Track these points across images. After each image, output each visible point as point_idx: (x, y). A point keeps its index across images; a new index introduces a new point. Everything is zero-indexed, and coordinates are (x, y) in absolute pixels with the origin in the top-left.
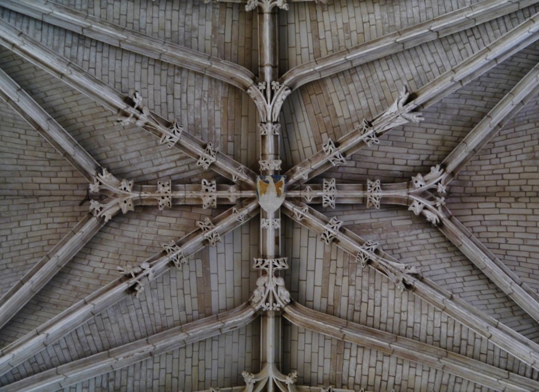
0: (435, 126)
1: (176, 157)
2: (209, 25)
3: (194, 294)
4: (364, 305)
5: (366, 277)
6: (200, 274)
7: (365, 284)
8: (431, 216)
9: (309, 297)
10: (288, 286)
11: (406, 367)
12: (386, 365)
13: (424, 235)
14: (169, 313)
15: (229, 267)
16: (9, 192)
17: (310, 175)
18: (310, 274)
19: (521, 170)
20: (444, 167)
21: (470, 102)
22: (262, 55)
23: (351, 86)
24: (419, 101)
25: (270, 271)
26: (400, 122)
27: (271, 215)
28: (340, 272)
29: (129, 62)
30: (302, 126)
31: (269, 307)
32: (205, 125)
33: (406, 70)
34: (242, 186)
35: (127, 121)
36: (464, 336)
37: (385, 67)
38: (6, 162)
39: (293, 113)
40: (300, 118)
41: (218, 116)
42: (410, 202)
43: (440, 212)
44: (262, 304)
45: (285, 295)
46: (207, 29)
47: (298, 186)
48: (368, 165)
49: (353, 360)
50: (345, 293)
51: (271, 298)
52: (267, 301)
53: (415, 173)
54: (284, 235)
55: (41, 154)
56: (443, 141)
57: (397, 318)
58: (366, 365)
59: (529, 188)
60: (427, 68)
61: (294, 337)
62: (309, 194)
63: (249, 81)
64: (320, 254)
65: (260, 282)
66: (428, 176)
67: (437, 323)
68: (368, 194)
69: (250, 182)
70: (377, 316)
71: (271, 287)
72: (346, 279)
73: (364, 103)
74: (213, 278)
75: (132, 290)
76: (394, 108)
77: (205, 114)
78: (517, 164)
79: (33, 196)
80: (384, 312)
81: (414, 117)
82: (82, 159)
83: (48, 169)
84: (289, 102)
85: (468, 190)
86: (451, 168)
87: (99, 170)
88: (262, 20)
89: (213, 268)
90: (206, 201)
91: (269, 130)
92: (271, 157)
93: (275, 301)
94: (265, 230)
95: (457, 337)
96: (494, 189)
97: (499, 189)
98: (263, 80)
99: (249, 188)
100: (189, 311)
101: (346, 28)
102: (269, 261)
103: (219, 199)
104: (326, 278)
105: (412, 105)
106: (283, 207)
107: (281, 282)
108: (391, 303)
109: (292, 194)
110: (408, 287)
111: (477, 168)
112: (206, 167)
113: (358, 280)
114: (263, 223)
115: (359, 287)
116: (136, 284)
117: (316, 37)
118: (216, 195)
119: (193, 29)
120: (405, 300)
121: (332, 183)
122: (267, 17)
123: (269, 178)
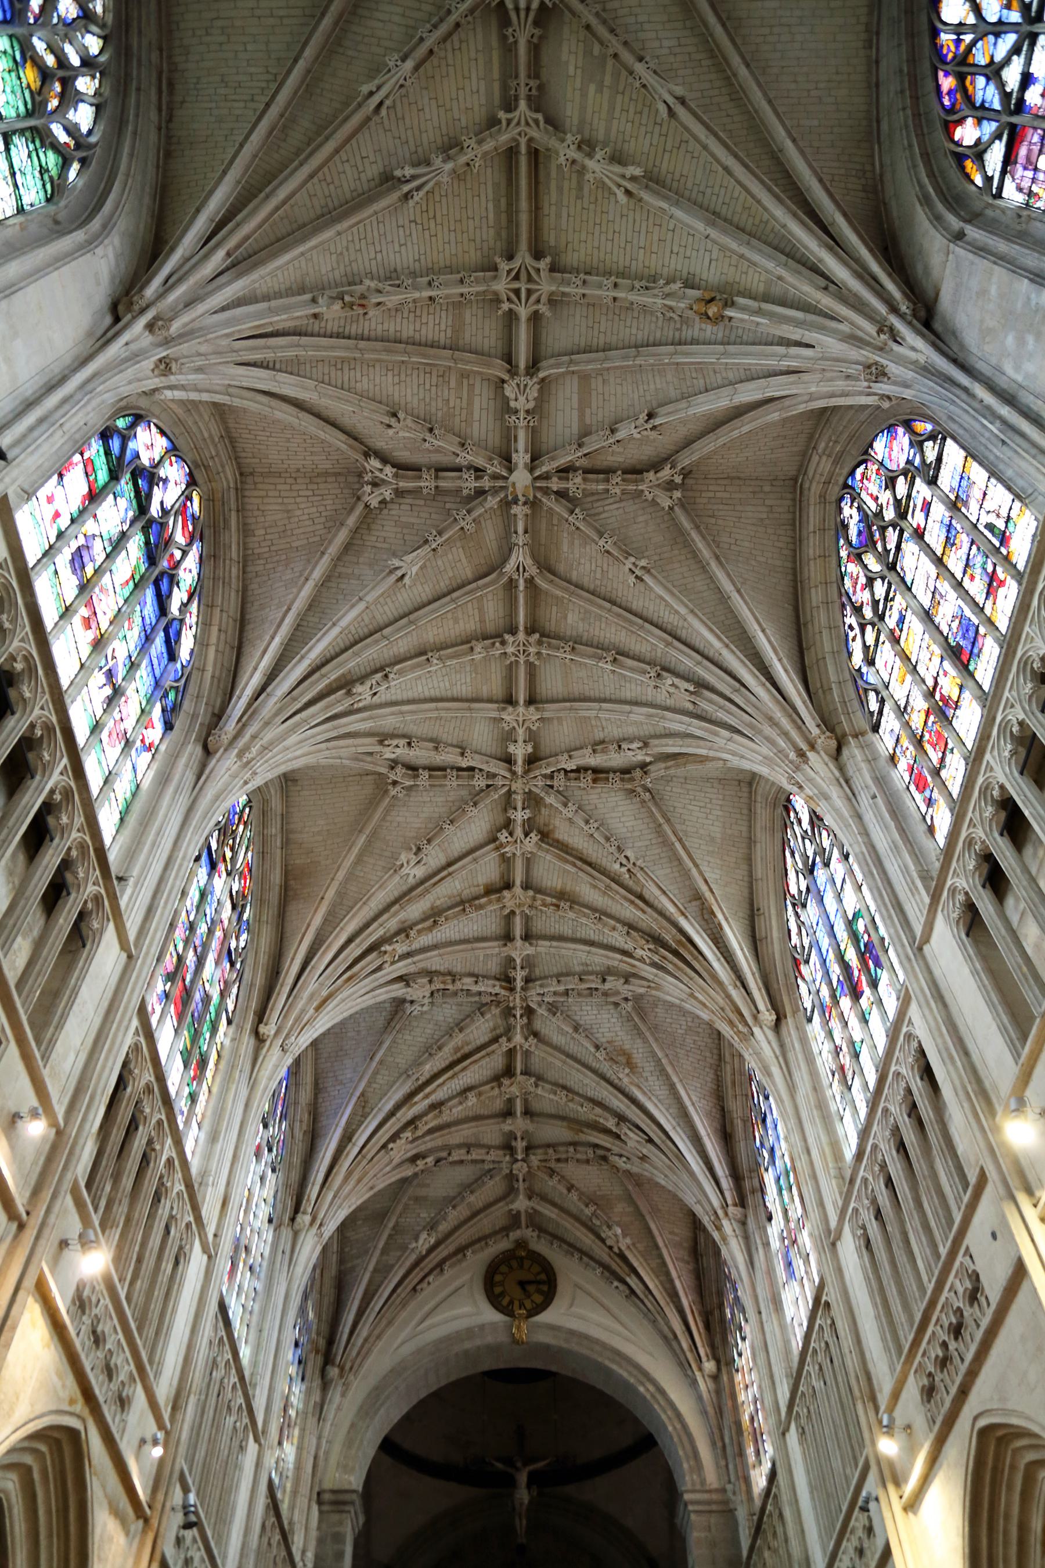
0: (378, 545)
1: (603, 516)
2: (569, 621)
3: (594, 393)
4: (434, 383)
5: (433, 410)
6: (588, 411)
7: (433, 404)
8: (375, 463)
9: (485, 383)
10: (506, 400)
11: (392, 330)
12: (411, 327)
13: (380, 444)
14: (619, 381)
15: (560, 413)
16: (752, 483)
17: (486, 499)
18: (485, 406)
19: (298, 500)
20: (367, 506)
21: (350, 571)
22: (526, 597)
23: (451, 574)
24: (393, 578)
25: (522, 415)
26: (408, 558)
27: (521, 465)
28: (457, 413)
29: (636, 605)
30: (493, 537)
31: (524, 380)
32: (576, 542)
33: (405, 595)
34: (546, 491)
35: (643, 563)
36: (339, 373)
37: (423, 595)
38: (750, 514)
39: (500, 548)
40: (494, 543)
41: (565, 549)
42: (396, 476)
43: (368, 467)
44: (530, 383)
45: (509, 391)
46: (572, 618)
47: (495, 491)
48: (435, 504)
49: (443, 327)
50: (452, 392)
51: (522, 389)
52: (526, 386)
53: (392, 501)
54: (509, 441)
55: (720, 522)
56: (369, 529)
57: (403, 376)
58: (431, 324)
59: (289, 481)
60: (388, 600)
61: (500, 343)
62: (486, 483)
63: (538, 581)
64: (476, 425)
65: (531, 405)
66: (380, 499)
67: (365, 379)
68: (433, 484)
69: (539, 495)
70: (422, 375)
71: (522, 399)
72: (452, 405)
73: (440, 563)
74: (576, 405)
75: (650, 416)
76: (415, 569)
77: (576, 551)
78: (302, 506)
79: (732, 478)
80: (415, 381)
81: (396, 563)
82: (686, 524)
83: (716, 507)
84: (505, 560)
85: (342, 479)
86: (360, 507)
87: (671, 508)
88: (526, 623)
89: (575, 414)
90: (578, 480)
91: (521, 539)
92: (520, 516)
93: (518, 385)
94: (526, 451)
95: (346, 371)
96: (319, 480)
97: (315, 480)
98: (526, 581)
99: (540, 488)
100: (600, 378)
101: (456, 621)
102: (522, 423)
103: (567, 479)
104: (470, 403)
105: (399, 573)
106: (510, 471)
107: (512, 404)
108: (409, 391)
109: (500, 483)
110: (395, 415)
111: (337, 501)
112: (577, 511)
113: (440, 405)
114: (528, 458)
115: (440, 400)
116: (646, 422)
117: (481, 609)
118: (570, 485)
119: (583, 620)
120: (396, 395)
121: (465, 492)
122: (521, 628)
123: (522, 499)
